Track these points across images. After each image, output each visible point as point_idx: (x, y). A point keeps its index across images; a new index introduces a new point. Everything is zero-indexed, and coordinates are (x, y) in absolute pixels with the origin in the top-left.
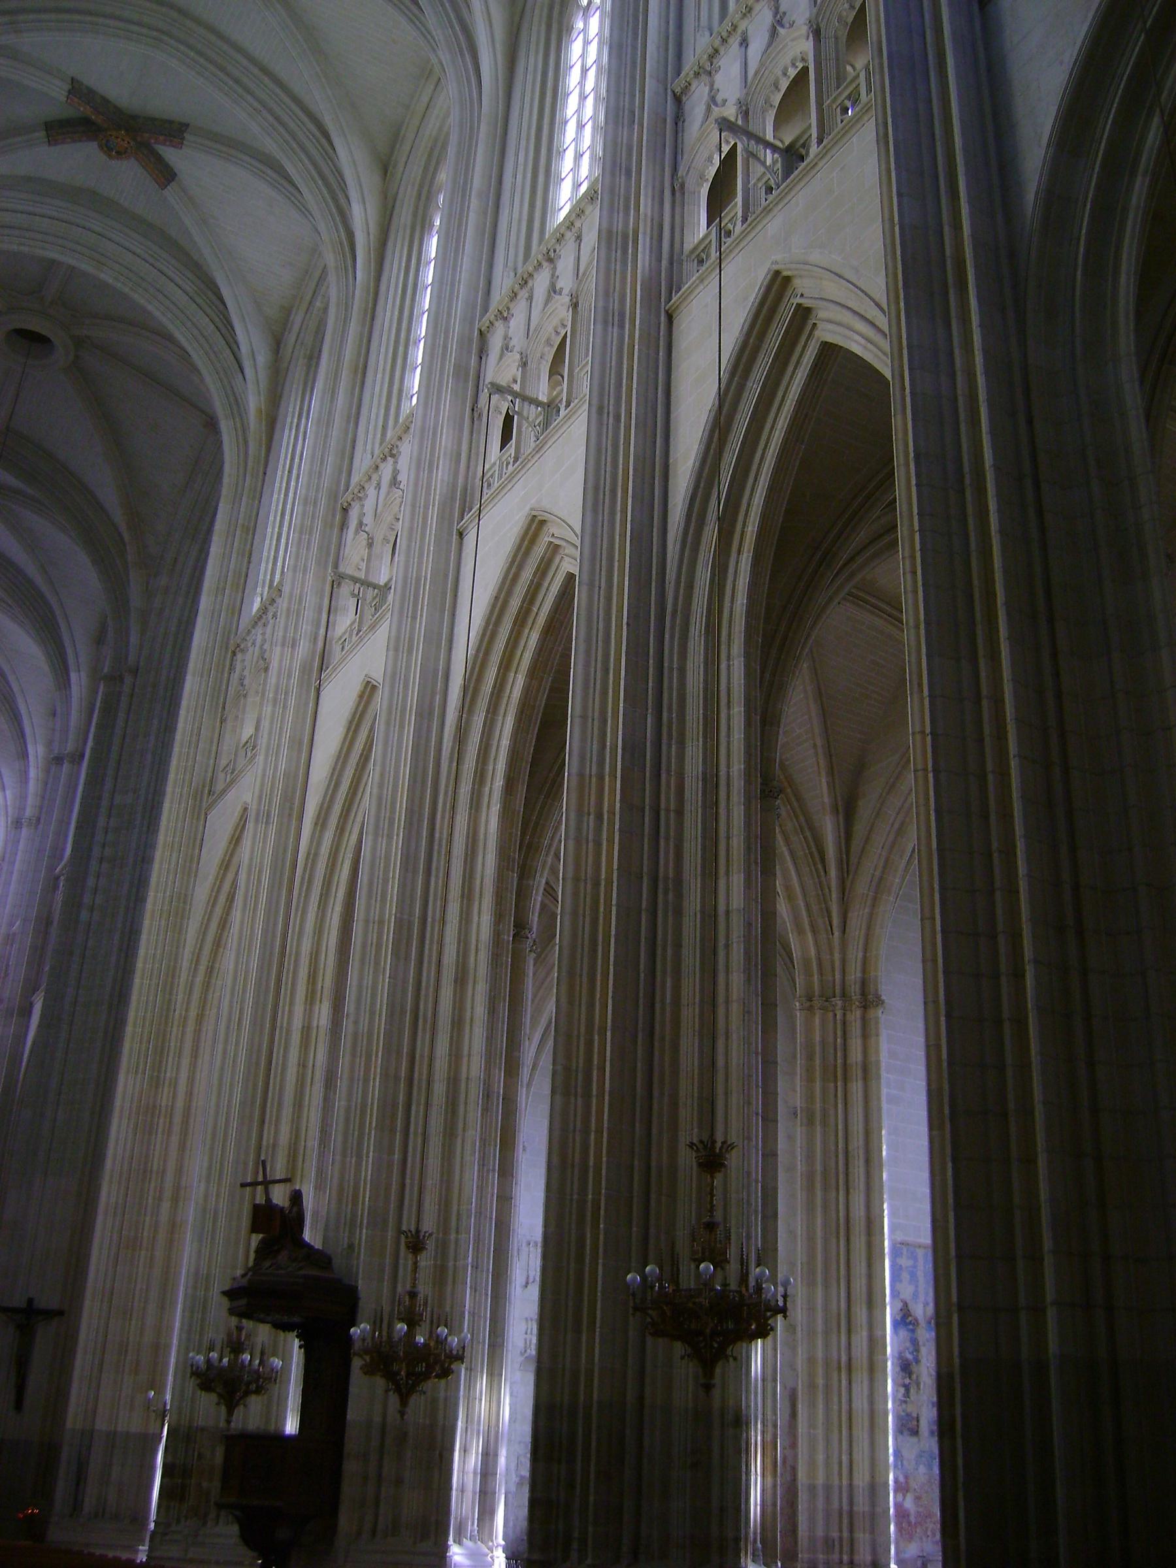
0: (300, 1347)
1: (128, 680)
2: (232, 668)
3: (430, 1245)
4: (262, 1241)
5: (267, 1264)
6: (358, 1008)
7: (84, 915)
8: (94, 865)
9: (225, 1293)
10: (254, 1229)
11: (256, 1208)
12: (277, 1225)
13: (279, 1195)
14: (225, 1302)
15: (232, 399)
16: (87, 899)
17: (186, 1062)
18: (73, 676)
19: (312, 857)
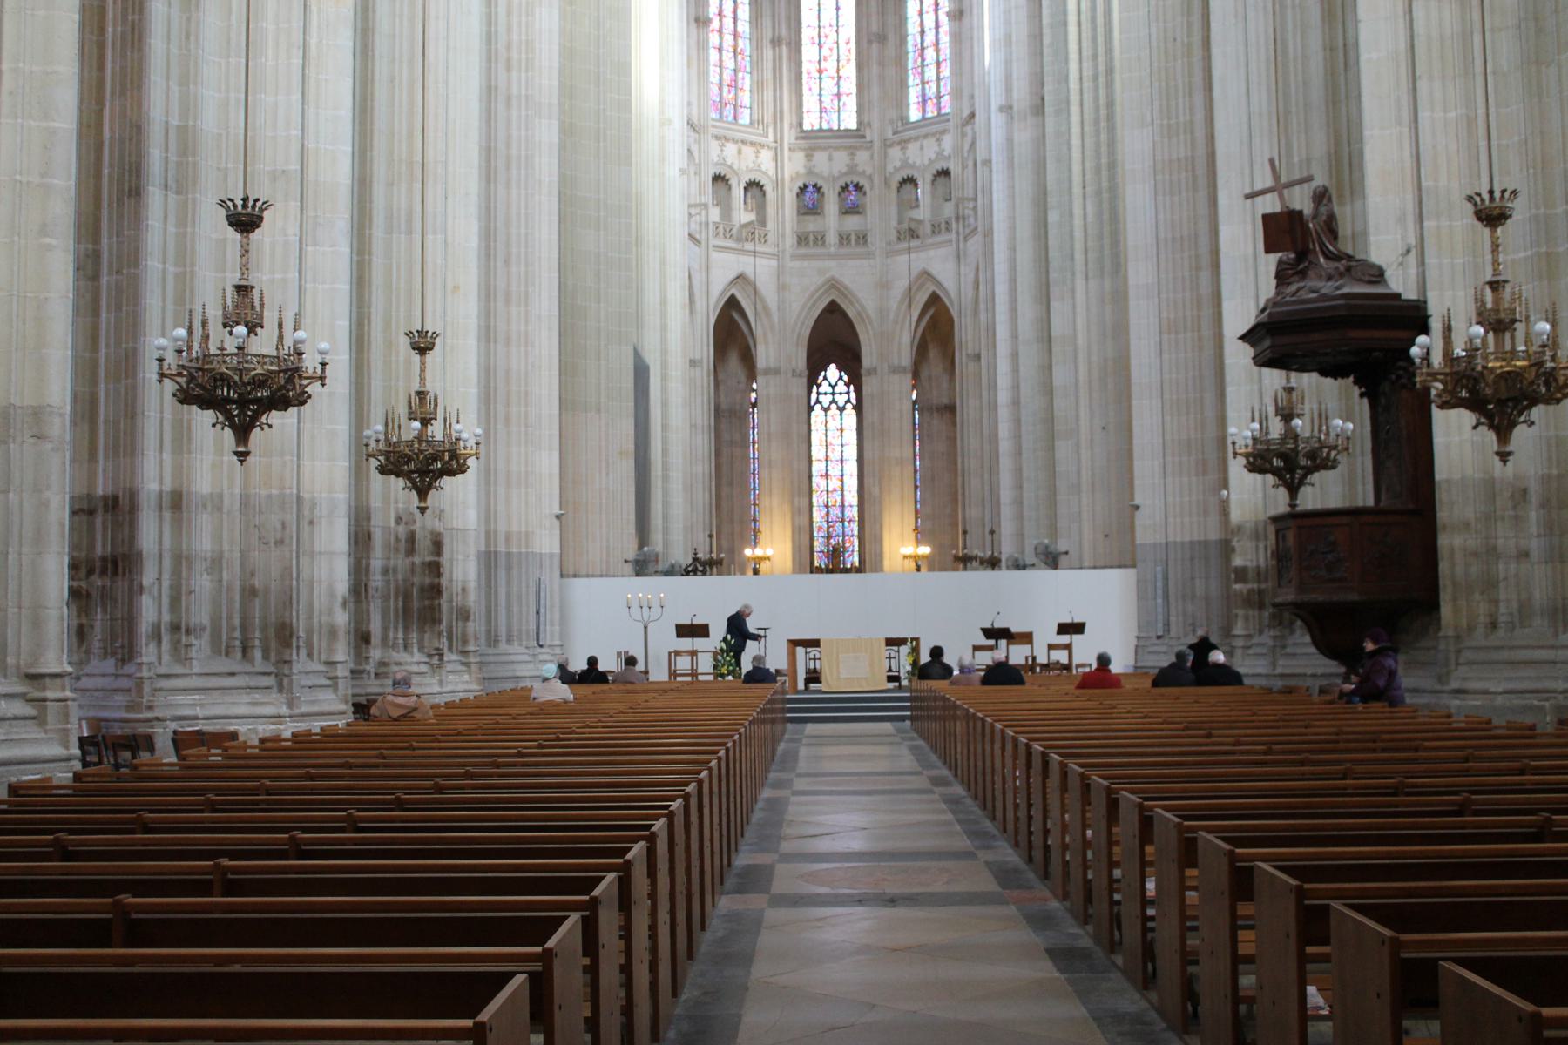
0: (1362, 395)
4: (1280, 262)
9: (1243, 338)
10: (1268, 250)
11: (1267, 219)
13: (1301, 200)
14: (1248, 351)
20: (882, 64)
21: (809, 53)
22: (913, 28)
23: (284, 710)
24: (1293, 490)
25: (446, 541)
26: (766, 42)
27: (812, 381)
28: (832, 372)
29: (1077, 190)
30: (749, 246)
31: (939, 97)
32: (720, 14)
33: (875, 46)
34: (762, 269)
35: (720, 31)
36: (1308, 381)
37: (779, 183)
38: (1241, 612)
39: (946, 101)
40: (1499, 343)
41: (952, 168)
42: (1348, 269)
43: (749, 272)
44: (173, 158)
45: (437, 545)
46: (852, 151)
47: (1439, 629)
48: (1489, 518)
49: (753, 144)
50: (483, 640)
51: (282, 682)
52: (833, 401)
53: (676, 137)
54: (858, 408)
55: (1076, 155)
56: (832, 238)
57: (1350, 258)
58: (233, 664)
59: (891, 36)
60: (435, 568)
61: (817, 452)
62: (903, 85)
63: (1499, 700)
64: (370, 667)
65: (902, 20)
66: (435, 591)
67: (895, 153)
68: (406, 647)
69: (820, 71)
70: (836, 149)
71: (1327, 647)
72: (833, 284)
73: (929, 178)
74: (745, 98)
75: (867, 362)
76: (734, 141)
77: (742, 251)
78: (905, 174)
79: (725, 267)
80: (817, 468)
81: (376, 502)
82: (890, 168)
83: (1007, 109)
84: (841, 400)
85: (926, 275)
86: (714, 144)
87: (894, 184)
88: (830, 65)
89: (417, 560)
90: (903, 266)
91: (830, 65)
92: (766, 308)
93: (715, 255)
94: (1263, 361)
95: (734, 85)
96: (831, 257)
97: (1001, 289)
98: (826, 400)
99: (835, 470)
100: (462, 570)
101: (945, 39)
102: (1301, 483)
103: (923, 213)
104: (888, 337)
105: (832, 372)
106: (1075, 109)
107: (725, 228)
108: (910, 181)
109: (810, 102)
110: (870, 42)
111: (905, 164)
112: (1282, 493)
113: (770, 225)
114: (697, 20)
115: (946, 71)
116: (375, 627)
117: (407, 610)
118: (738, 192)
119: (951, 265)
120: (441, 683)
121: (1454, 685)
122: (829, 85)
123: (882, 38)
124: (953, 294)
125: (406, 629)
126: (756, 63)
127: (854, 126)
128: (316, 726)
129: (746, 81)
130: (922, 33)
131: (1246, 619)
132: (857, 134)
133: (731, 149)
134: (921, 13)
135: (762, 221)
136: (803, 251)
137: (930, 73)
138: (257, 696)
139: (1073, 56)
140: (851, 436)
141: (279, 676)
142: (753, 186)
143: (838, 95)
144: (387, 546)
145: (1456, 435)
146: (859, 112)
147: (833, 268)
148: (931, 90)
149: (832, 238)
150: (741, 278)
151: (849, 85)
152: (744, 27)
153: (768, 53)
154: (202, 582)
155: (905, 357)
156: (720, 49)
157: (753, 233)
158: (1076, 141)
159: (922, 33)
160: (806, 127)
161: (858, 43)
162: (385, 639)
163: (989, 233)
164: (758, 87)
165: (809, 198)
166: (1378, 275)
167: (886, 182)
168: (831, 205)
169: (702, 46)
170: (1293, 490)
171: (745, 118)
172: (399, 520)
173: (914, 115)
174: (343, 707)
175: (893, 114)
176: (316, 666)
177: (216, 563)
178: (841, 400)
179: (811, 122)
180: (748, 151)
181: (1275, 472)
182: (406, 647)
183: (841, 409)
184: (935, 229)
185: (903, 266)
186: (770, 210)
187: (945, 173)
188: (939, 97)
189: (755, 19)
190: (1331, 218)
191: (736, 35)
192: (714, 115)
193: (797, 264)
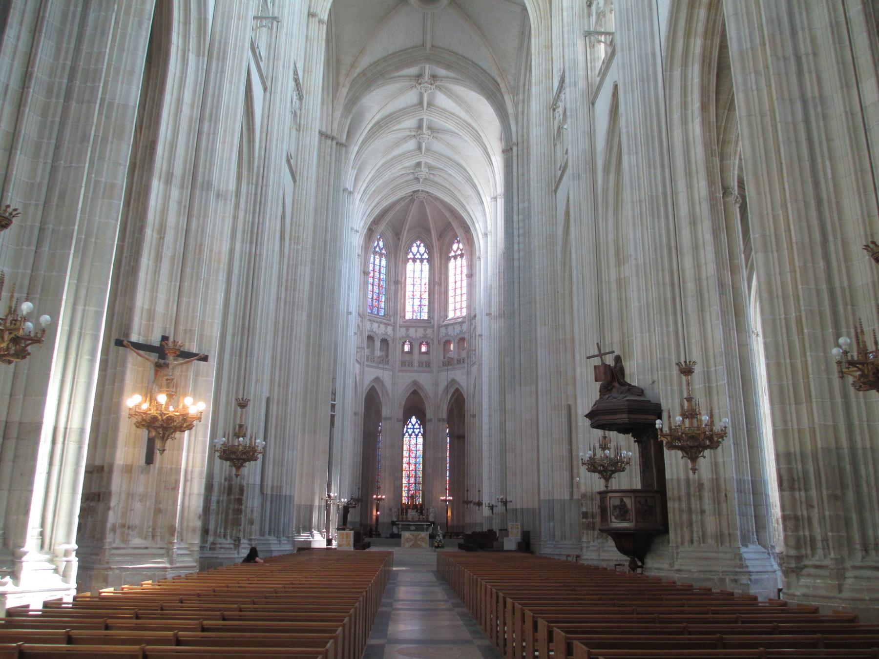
1: (515, 149)
2: (554, 118)
3: (698, 369)
6: (636, 250)
7: (516, 263)
8: (516, 239)
9: (586, 416)
12: (612, 376)
13: (610, 361)
14: (588, 422)
16: (516, 256)
17: (567, 316)
18: (493, 158)
19: (605, 190)
21: (409, 288)
22: (451, 280)
23: (168, 565)
24: (607, 479)
25: (245, 489)
27: (405, 422)
28: (414, 420)
29: (517, 349)
30: (381, 366)
31: (461, 308)
32: (374, 270)
34: (386, 377)
35: (373, 277)
36: (613, 434)
37: (394, 340)
38: (585, 532)
40: (691, 423)
41: (467, 336)
42: (629, 390)
43: (381, 376)
45: (242, 491)
46: (425, 328)
47: (668, 542)
48: (688, 495)
49: (385, 324)
50: (258, 534)
51: (168, 552)
52: (413, 432)
53: (354, 319)
54: (424, 435)
55: (517, 335)
56: (416, 364)
57: (630, 385)
58: (148, 543)
60: (240, 501)
63: (695, 575)
64: (208, 545)
66: (239, 511)
67: (443, 330)
68: (225, 536)
70: (419, 327)
71: (622, 549)
72: (415, 383)
73: (456, 340)
75: (428, 416)
76: (377, 322)
77: (380, 368)
78: (446, 338)
79: (372, 373)
80: (405, 460)
81: (217, 471)
82: (441, 336)
83: (488, 315)
84: (417, 431)
85: (453, 381)
88: (418, 294)
89: (232, 497)
92: (386, 392)
93: (366, 369)
94: (595, 426)
95: (378, 300)
96: (416, 372)
97: (485, 388)
98: (410, 431)
99: (413, 461)
100: (253, 503)
101: (465, 284)
102: (610, 477)
104: (438, 405)
105: (414, 420)
106: (517, 316)
107: (371, 358)
109: (408, 308)
110: (434, 285)
111: (447, 334)
112: (602, 481)
113: (390, 357)
114: (364, 272)
115: (465, 297)
116: (212, 527)
117: (226, 520)
118: (378, 344)
120: (238, 553)
121: (676, 567)
122: (417, 302)
124: (465, 389)
125: (226, 528)
126: (387, 291)
127: (426, 318)
128: (183, 572)
131: (588, 535)
132: (428, 321)
133: (375, 325)
135: (387, 356)
136: (403, 368)
137: (458, 298)
139: (517, 295)
140: (420, 447)
142: (384, 341)
143: (420, 305)
144: (220, 490)
145: (674, 463)
146: (429, 313)
147: (416, 377)
148: (458, 306)
149: (416, 364)
150: (377, 379)
151: (425, 302)
153: (392, 287)
154: (138, 506)
155: (445, 415)
156: (373, 285)
157: (385, 360)
158: (517, 330)
161: (429, 285)
162: (215, 532)
163: (480, 365)
164: (387, 301)
166: (641, 392)
169: (366, 283)
170: (607, 479)
172: (226, 479)
173: (451, 315)
174: (195, 564)
175: (442, 314)
176: (183, 545)
177: (144, 497)
178: (417, 431)
179: (408, 316)
180: (382, 326)
181: (600, 472)
182: (225, 536)
183: (417, 435)
184: (459, 362)
185: (444, 378)
186: (390, 350)
188: (461, 308)
190: (622, 371)
191: (379, 279)
193: (401, 374)
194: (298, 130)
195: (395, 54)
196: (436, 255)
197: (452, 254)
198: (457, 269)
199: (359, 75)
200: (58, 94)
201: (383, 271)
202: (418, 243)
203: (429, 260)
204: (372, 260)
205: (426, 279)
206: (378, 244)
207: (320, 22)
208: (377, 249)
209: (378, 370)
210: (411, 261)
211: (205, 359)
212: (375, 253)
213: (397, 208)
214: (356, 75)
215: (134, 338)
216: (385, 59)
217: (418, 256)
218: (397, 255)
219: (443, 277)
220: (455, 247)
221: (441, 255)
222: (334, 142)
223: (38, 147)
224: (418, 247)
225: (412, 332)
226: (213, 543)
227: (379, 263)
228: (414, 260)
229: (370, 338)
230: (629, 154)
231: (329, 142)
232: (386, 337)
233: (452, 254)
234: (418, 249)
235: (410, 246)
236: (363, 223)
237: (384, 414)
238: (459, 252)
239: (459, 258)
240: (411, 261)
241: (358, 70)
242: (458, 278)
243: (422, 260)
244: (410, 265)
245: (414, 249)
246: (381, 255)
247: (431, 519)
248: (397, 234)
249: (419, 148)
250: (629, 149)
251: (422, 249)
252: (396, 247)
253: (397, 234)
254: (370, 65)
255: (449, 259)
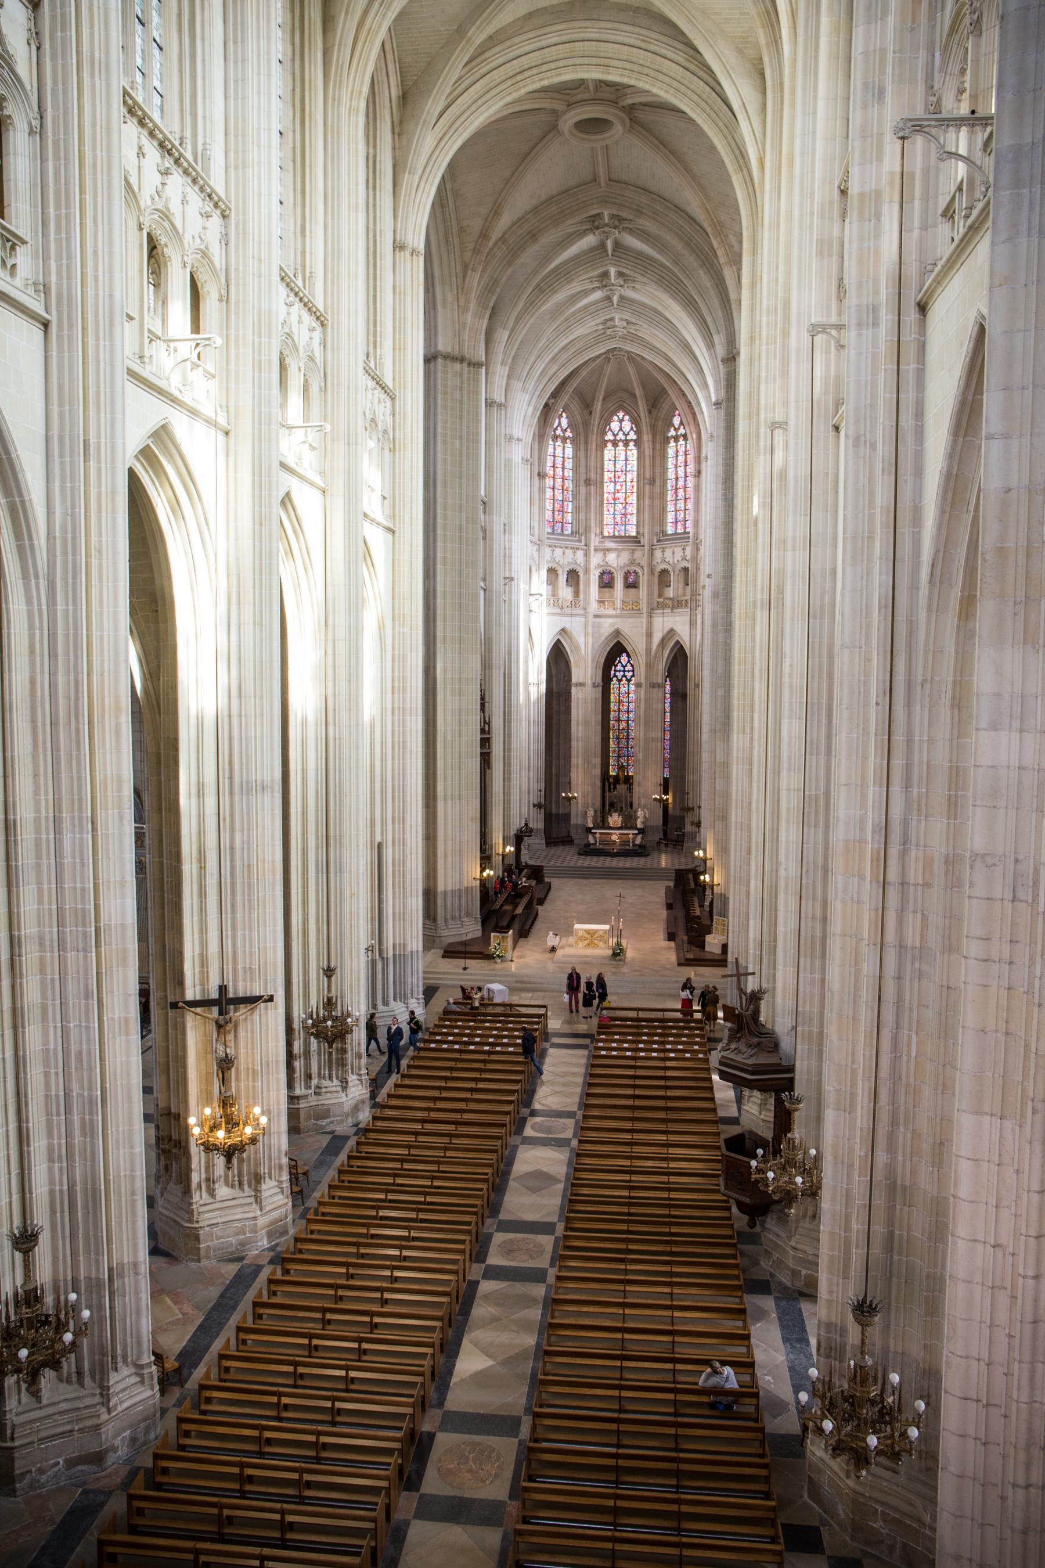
5: (733, 1046)
6: (787, 858)
15: (737, 152)
20: (652, 498)
21: (609, 487)
22: (671, 474)
26: (582, 483)
33: (647, 487)
34: (576, 626)
37: (587, 570)
39: (688, 523)
43: (568, 627)
44: (197, 970)
59: (658, 481)
61: (613, 706)
62: (664, 510)
64: (312, 1091)
65: (664, 470)
67: (658, 554)
68: (330, 1078)
69: (615, 499)
72: (617, 632)
74: (569, 517)
85: (672, 631)
86: (548, 550)
87: (657, 574)
90: (663, 623)
91: (621, 496)
95: (562, 511)
99: (624, 717)
103: (670, 592)
108: (664, 572)
109: (608, 519)
114: (539, 474)
118: (562, 578)
119: (687, 627)
123: (652, 482)
125: (330, 1070)
126: (575, 496)
127: (634, 534)
129: (569, 507)
130: (677, 479)
132: (636, 540)
133: (559, 552)
134: (676, 467)
137: (681, 505)
138: (246, 1208)
141: (256, 1197)
146: (638, 526)
151: (632, 509)
152: (569, 473)
153: (583, 490)
159: (677, 479)
160: (606, 534)
161: (638, 482)
164: (576, 510)
165: (606, 582)
167: (652, 571)
168: (619, 584)
169: (542, 491)
171: (568, 530)
173: (670, 530)
175: (657, 529)
176: (274, 1183)
180: (569, 552)
182: (330, 1078)
183: (629, 681)
187: (686, 569)
189: (576, 469)
191: (563, 478)
192: (549, 530)
194: (392, 450)
195: (550, 200)
196: (646, 437)
197: (672, 433)
198: (677, 456)
199: (495, 244)
200: (52, 947)
201: (569, 464)
202: (621, 414)
203: (638, 443)
204: (550, 450)
205: (633, 475)
206: (560, 424)
207: (414, 252)
208: (559, 432)
209: (565, 618)
210: (609, 445)
211: (271, 999)
212: (555, 438)
213: (584, 373)
214: (491, 244)
215: (190, 995)
216: (535, 210)
217: (621, 436)
218: (588, 436)
219: (658, 470)
220: (676, 421)
221: (654, 435)
222: (465, 365)
223: (44, 1008)
224: (621, 421)
225: (612, 557)
226: (318, 1087)
227: (561, 453)
228: (615, 444)
229: (552, 572)
230: (790, 718)
231: (457, 366)
232: (575, 567)
233: (672, 433)
234: (621, 425)
235: (608, 422)
236: (531, 409)
237: (574, 680)
238: (682, 431)
239: (682, 442)
240: (609, 445)
241: (495, 236)
242: (681, 473)
243: (626, 443)
244: (609, 452)
245: (615, 425)
246: (564, 440)
247: (639, 825)
248: (587, 406)
249: (609, 298)
250: (791, 710)
251: (627, 425)
252: (586, 424)
253: (587, 406)
254: (514, 224)
255: (667, 440)
